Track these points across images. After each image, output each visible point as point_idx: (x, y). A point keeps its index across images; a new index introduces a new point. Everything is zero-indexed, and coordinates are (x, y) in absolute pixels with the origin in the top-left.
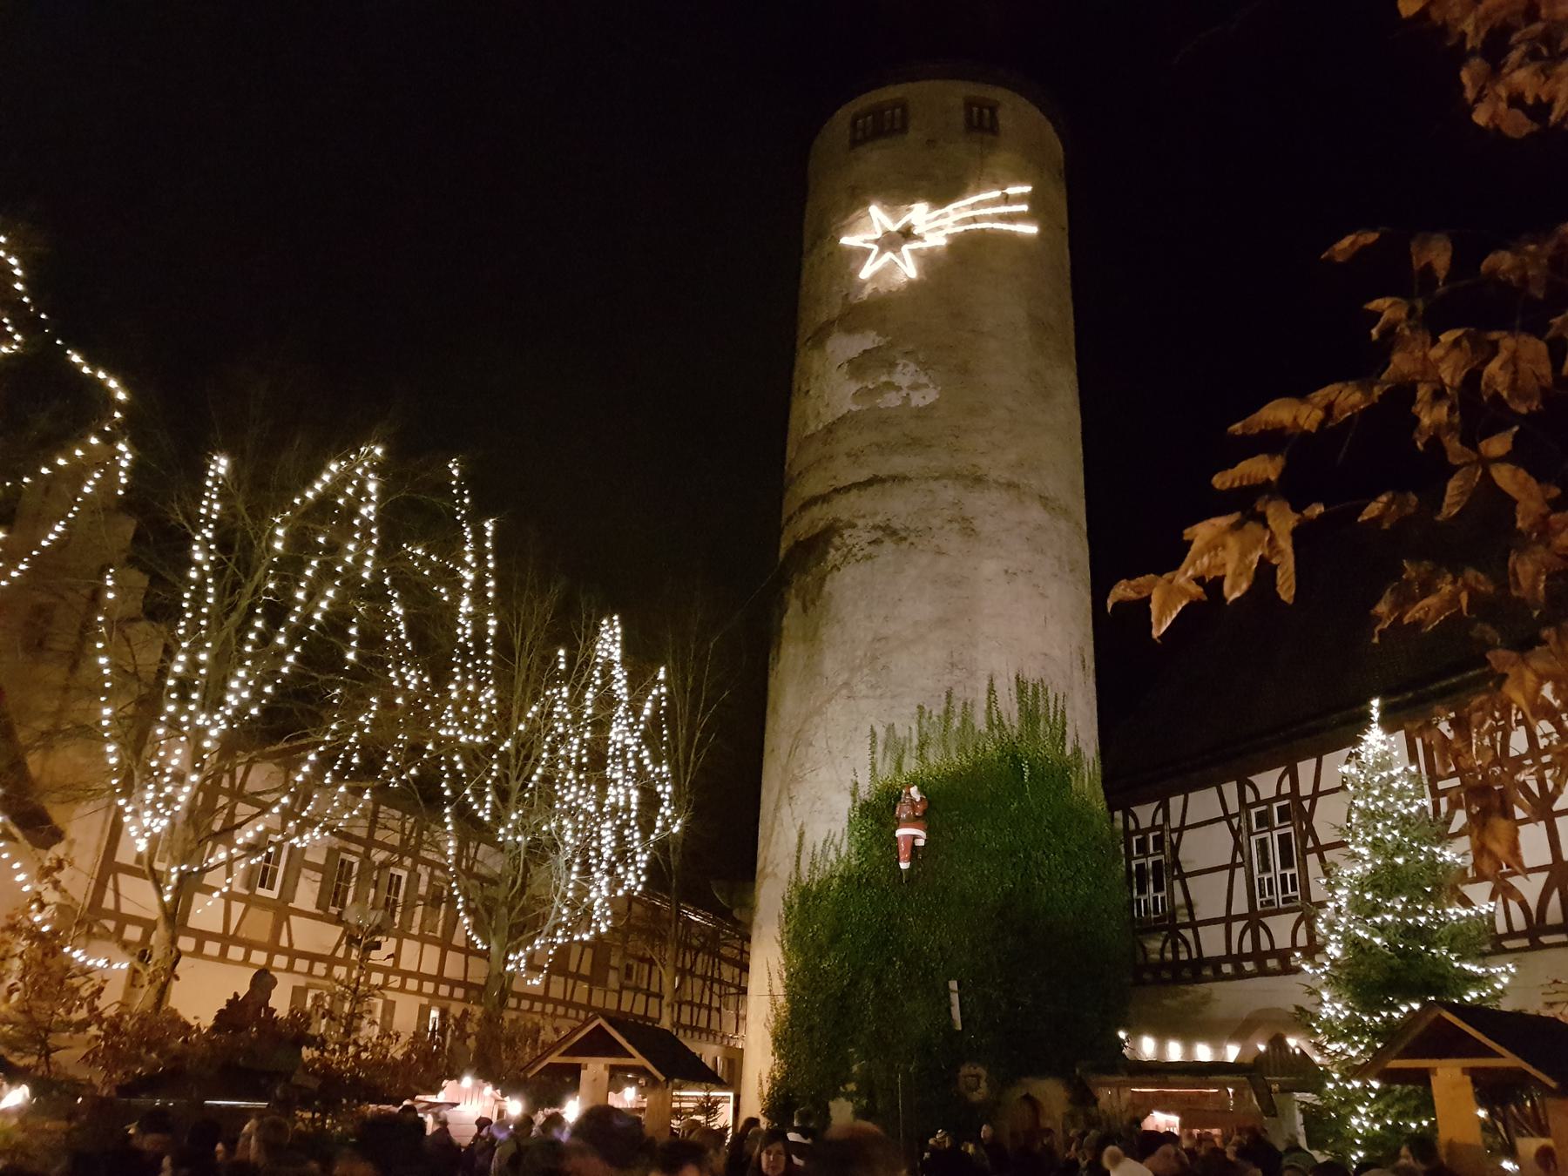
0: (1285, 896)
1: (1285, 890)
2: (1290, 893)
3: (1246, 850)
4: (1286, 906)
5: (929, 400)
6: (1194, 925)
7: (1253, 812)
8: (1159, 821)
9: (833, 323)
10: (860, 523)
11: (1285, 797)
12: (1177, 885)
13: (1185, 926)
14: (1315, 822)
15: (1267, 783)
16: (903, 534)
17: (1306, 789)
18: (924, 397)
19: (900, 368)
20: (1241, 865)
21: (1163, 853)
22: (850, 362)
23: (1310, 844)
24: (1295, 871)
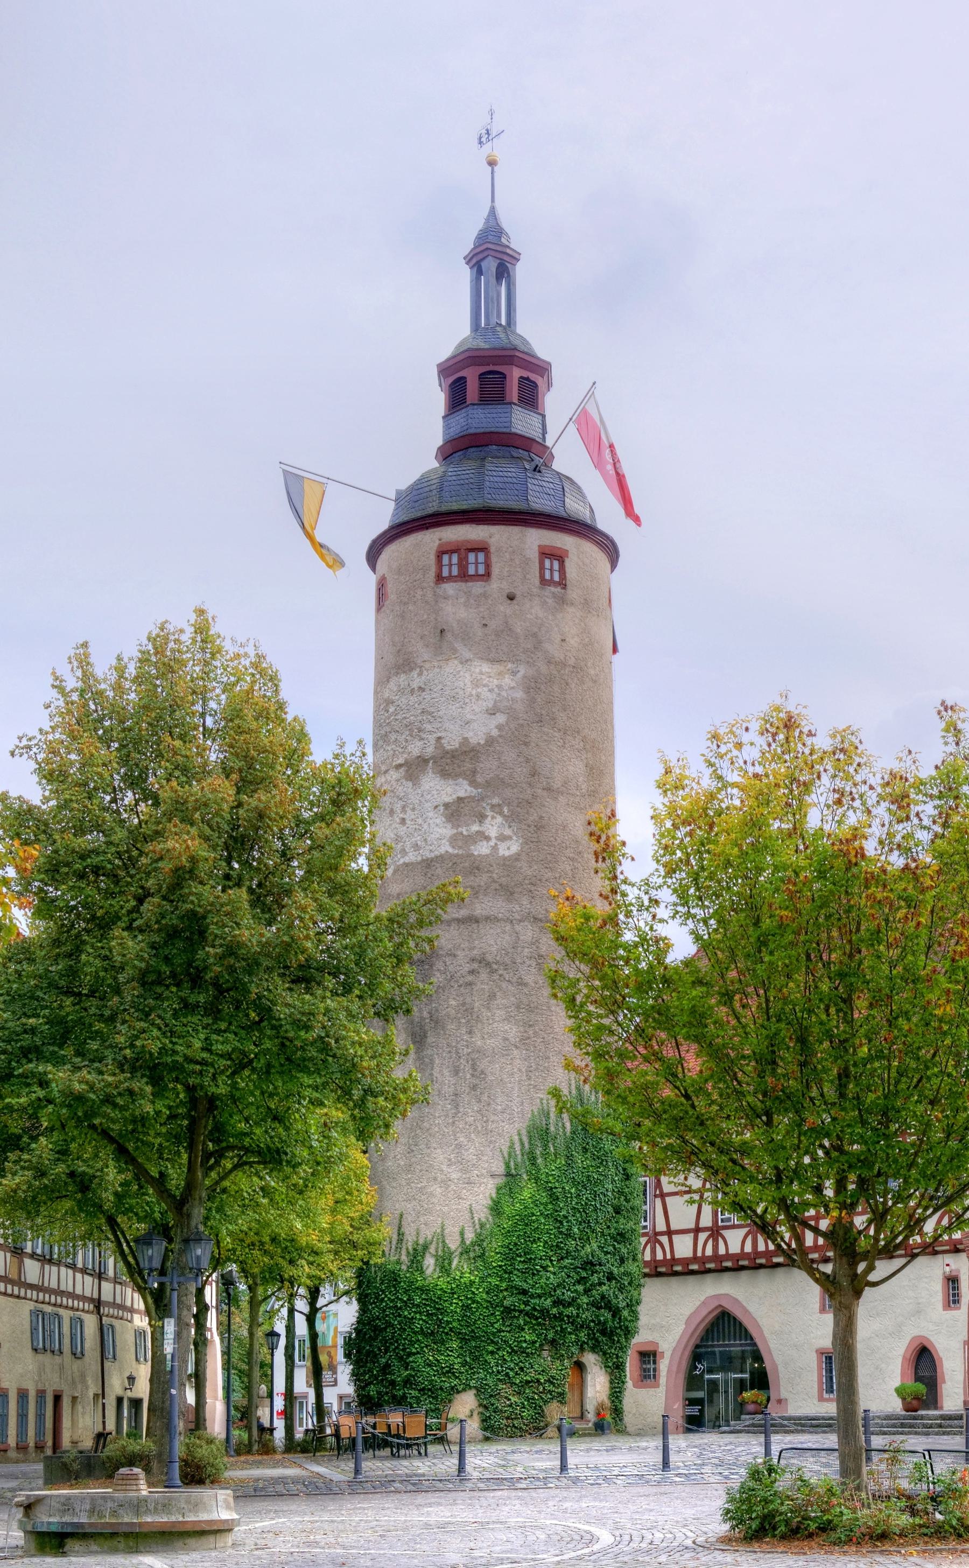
6: (670, 1233)
9: (426, 761)
16: (495, 966)
18: (509, 848)
19: (489, 818)
22: (446, 805)
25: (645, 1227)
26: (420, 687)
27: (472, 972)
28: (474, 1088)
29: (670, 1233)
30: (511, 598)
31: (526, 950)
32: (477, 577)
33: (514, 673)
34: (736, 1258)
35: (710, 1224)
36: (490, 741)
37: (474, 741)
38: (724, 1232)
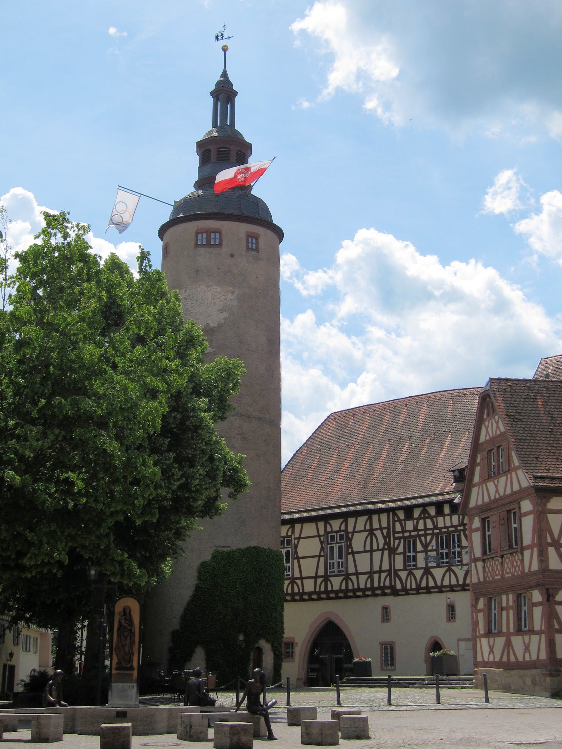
1: (339, 568)
2: (341, 569)
3: (326, 550)
7: (329, 535)
8: (290, 534)
11: (343, 531)
12: (296, 561)
14: (353, 543)
15: (336, 525)
17: (350, 529)
20: (323, 556)
21: (290, 548)
23: (350, 551)
24: (343, 560)
25: (288, 575)
26: (185, 298)
29: (302, 578)
30: (232, 256)
32: (215, 246)
33: (233, 293)
34: (336, 592)
35: (323, 574)
36: (220, 325)
37: (212, 325)
38: (330, 578)
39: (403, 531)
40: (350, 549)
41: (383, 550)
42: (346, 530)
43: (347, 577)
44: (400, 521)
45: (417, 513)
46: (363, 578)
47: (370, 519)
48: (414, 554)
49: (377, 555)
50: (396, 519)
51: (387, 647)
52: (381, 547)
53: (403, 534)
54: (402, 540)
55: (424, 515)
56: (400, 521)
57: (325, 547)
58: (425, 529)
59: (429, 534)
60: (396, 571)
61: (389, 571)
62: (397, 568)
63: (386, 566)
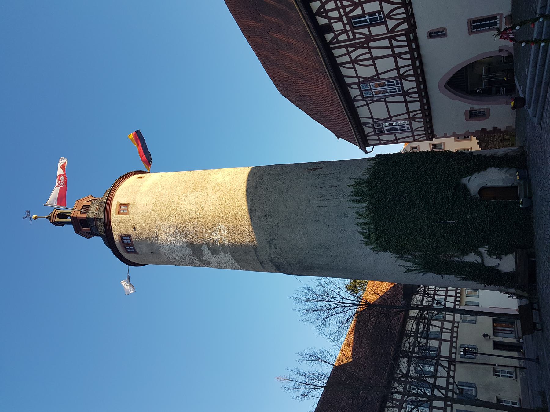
0: (396, 84)
1: (394, 85)
2: (395, 82)
3: (379, 98)
4: (400, 84)
5: (224, 228)
10: (269, 252)
13: (409, 116)
14: (368, 76)
15: (354, 92)
16: (272, 237)
17: (356, 80)
22: (213, 254)
23: (376, 77)
27: (276, 248)
28: (327, 248)
30: (134, 228)
31: (263, 223)
32: (131, 240)
39: (346, 31)
40: (374, 78)
41: (369, 48)
42: (358, 84)
43: (401, 77)
44: (336, 37)
45: (322, 21)
46: (401, 62)
47: (342, 64)
48: (367, 16)
49: (375, 53)
50: (335, 40)
51: (473, 26)
52: (367, 51)
53: (349, 31)
54: (355, 31)
55: (323, 12)
56: (336, 37)
57: (377, 98)
58: (337, 9)
59: (342, 3)
60: (389, 32)
61: (390, 39)
62: (386, 32)
63: (386, 43)
